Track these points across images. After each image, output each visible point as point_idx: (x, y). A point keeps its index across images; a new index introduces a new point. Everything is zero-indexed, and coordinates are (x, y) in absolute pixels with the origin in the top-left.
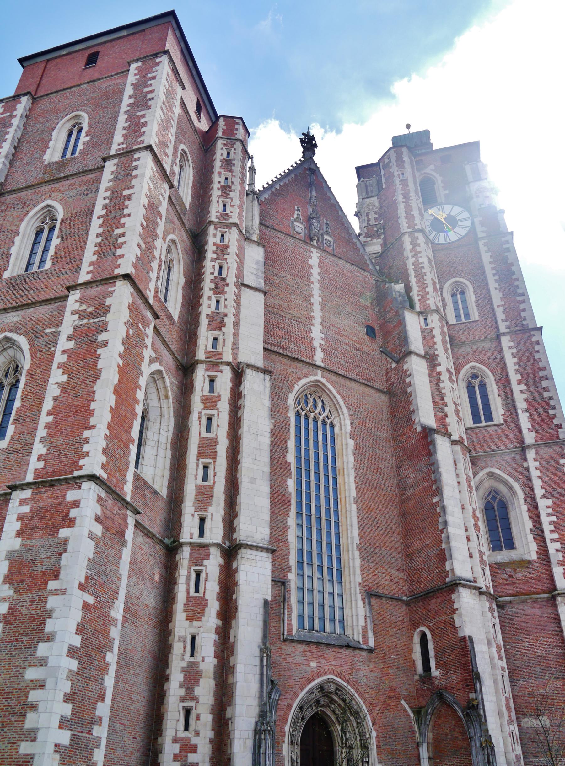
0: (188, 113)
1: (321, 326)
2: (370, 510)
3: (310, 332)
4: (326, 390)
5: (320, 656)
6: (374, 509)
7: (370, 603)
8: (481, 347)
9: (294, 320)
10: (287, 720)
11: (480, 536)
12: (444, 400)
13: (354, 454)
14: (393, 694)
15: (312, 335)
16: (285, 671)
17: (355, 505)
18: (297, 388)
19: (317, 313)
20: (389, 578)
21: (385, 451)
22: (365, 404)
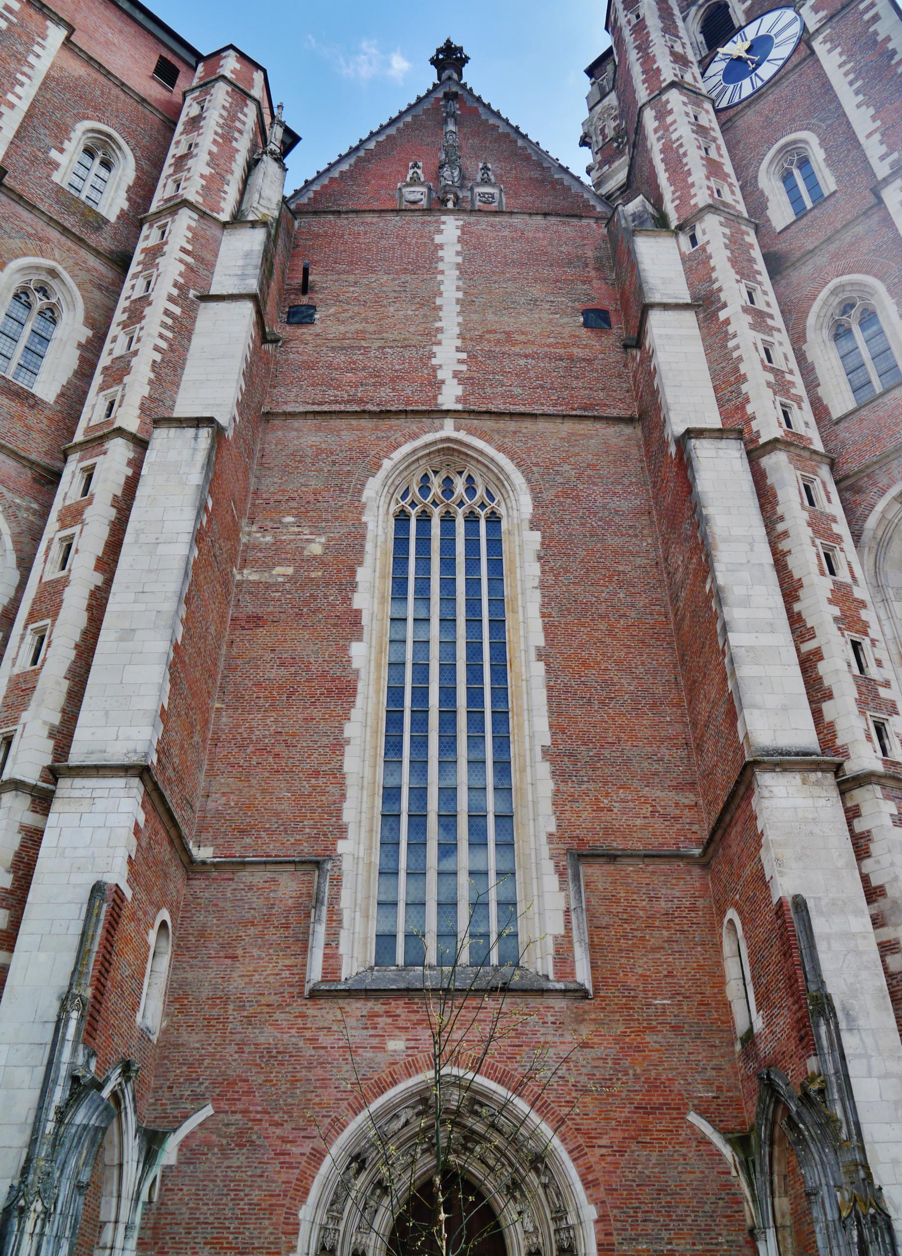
0: (109, 73)
2: (588, 667)
3: (430, 358)
4: (469, 452)
5: (419, 1022)
6: (598, 663)
7: (576, 877)
8: (848, 239)
10: (307, 1192)
11: (866, 643)
12: (738, 371)
13: (540, 558)
14: (657, 1100)
16: (309, 1068)
17: (541, 666)
18: (387, 464)
20: (647, 810)
21: (636, 536)
22: (578, 454)
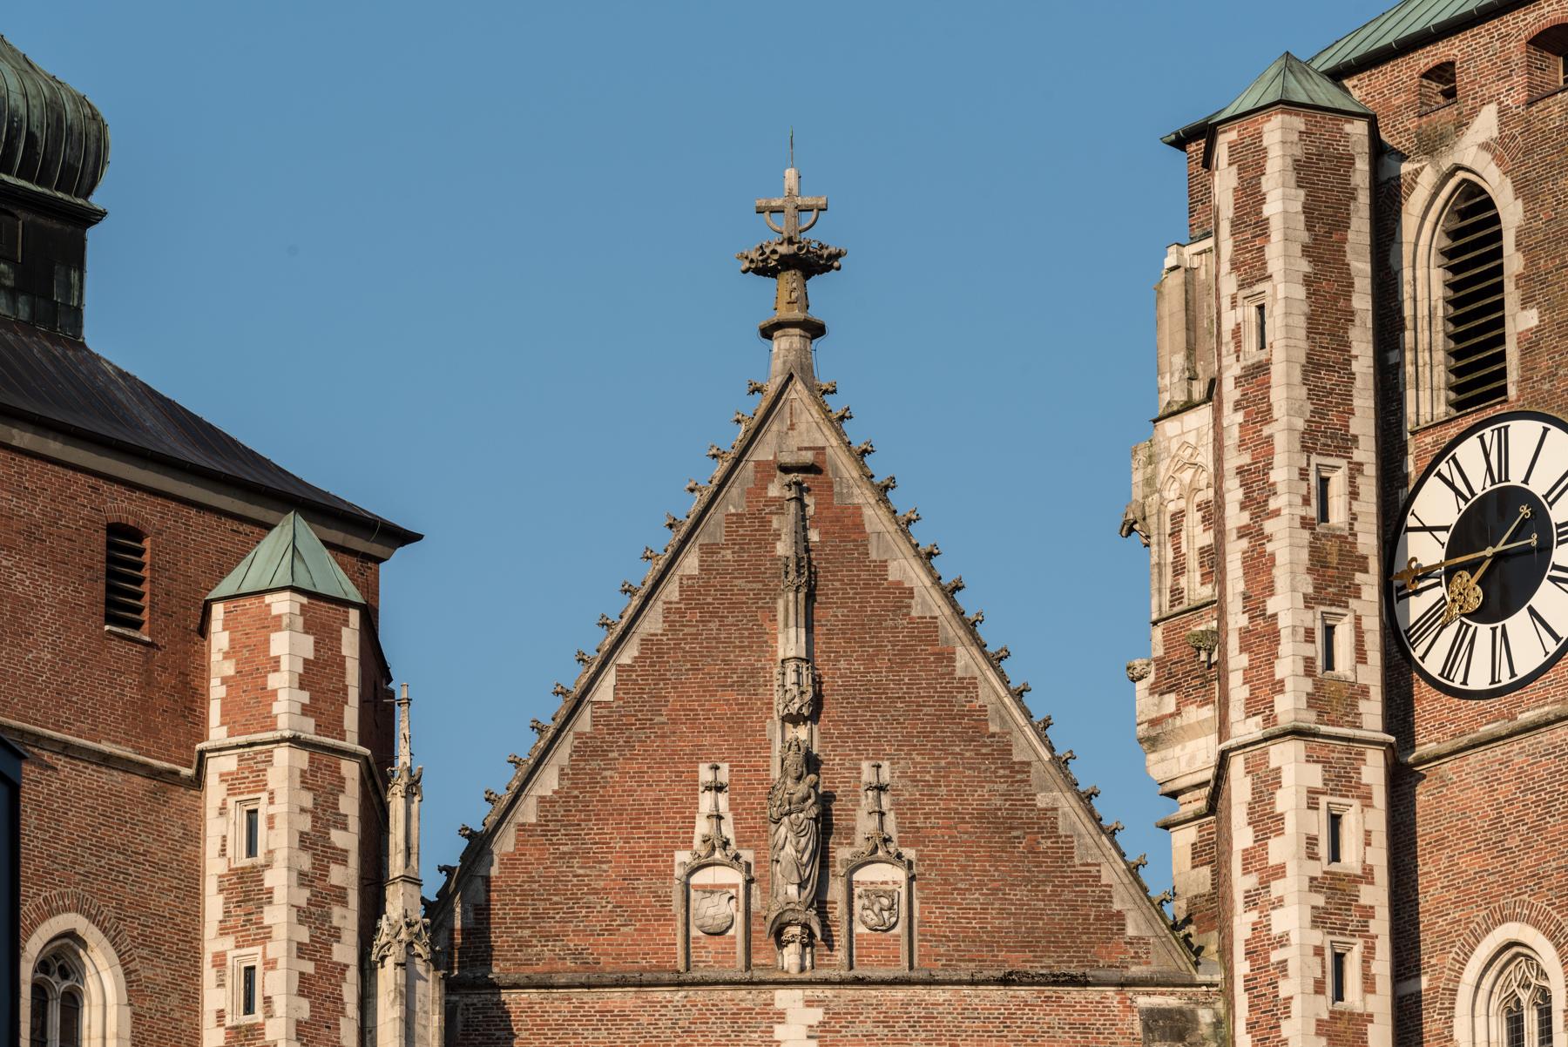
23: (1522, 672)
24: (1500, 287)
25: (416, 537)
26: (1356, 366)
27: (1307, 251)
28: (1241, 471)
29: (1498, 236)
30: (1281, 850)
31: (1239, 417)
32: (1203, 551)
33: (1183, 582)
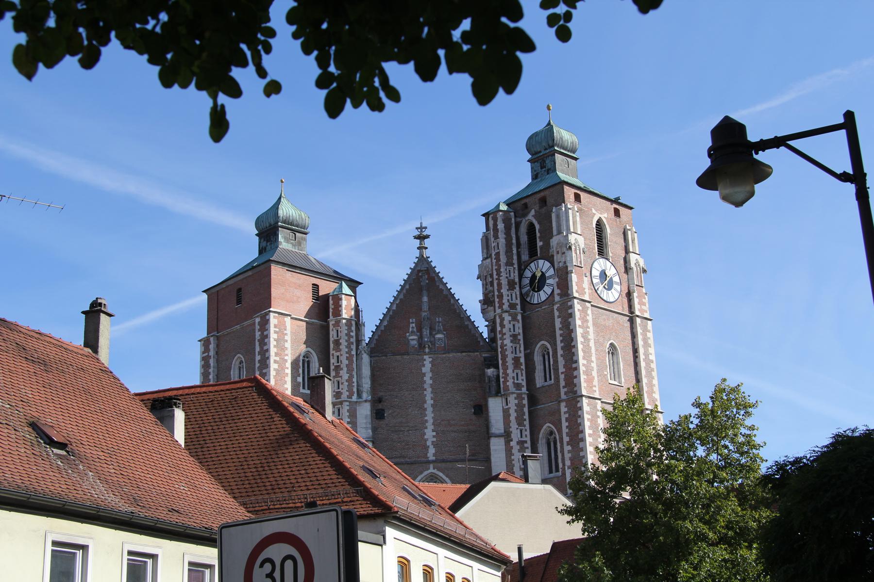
1: (433, 426)
9: (411, 430)
15: (426, 437)
19: (430, 416)
23: (542, 300)
24: (536, 238)
25: (362, 283)
26: (513, 252)
27: (505, 234)
28: (496, 269)
29: (535, 230)
30: (504, 331)
31: (495, 261)
32: (490, 282)
33: (487, 287)
